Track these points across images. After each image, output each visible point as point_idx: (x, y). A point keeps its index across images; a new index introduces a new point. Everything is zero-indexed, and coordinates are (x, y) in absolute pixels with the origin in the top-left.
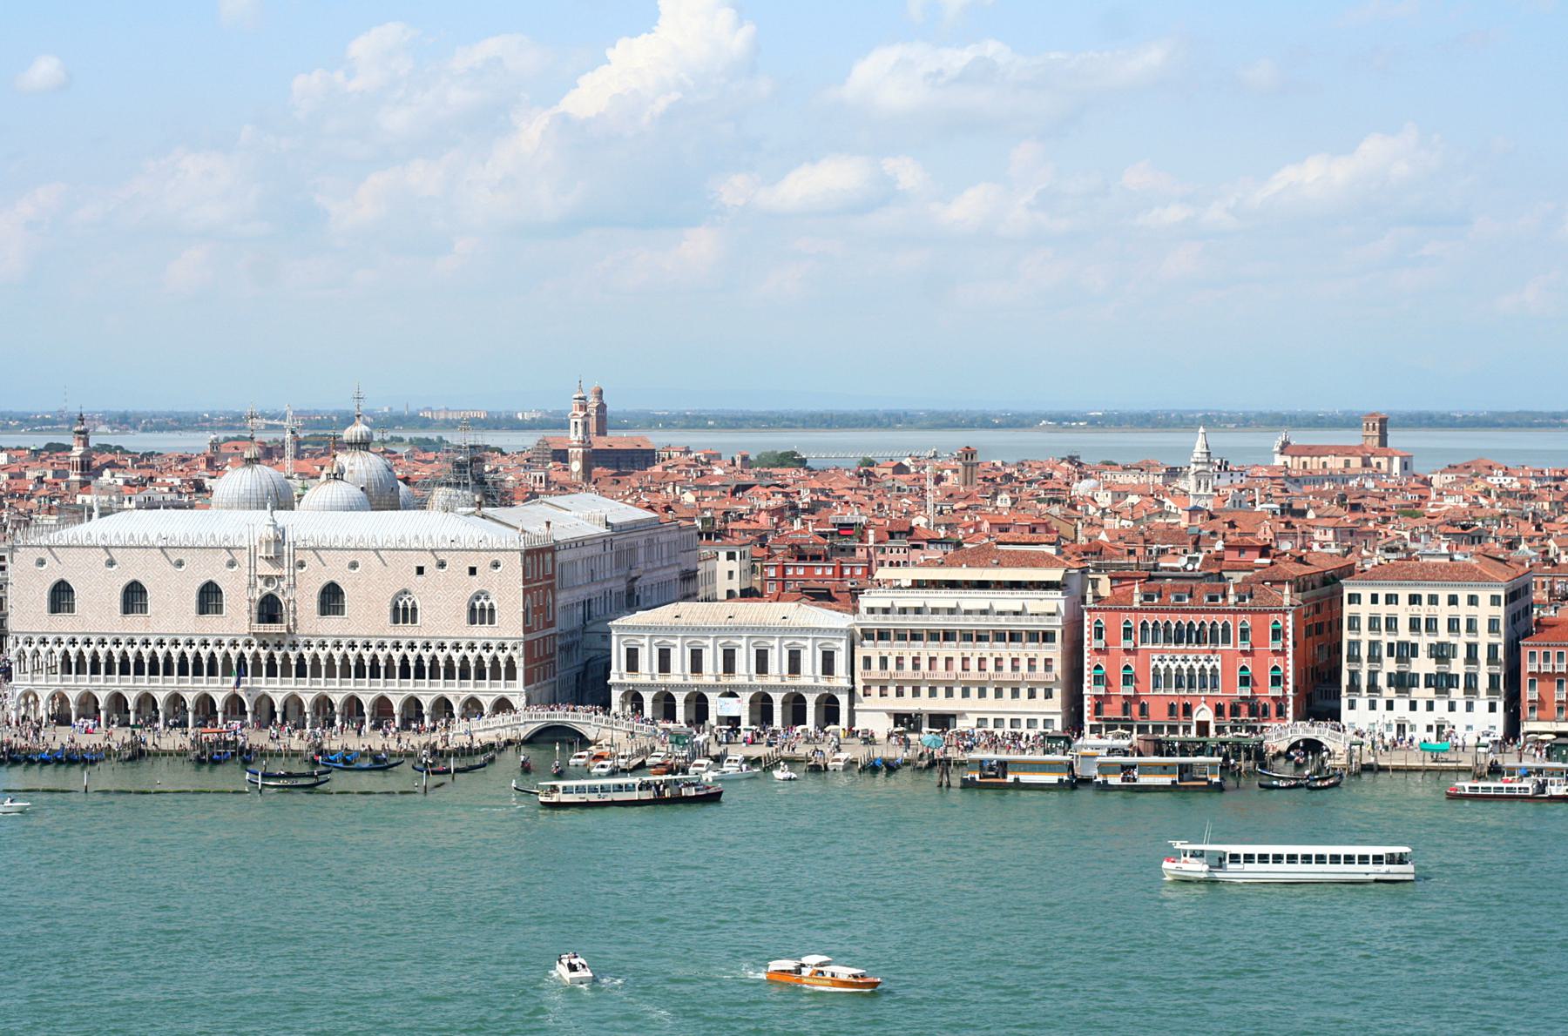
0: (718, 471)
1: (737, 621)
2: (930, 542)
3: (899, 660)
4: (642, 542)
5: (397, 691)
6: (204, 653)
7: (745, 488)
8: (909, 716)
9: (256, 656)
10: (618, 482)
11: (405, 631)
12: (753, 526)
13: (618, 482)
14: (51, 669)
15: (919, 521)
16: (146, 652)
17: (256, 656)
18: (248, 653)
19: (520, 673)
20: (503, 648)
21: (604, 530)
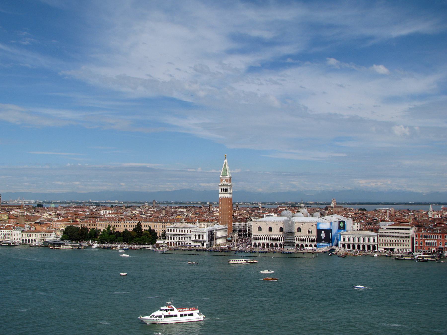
1: (360, 234)
3: (385, 240)
11: (310, 234)
14: (258, 239)
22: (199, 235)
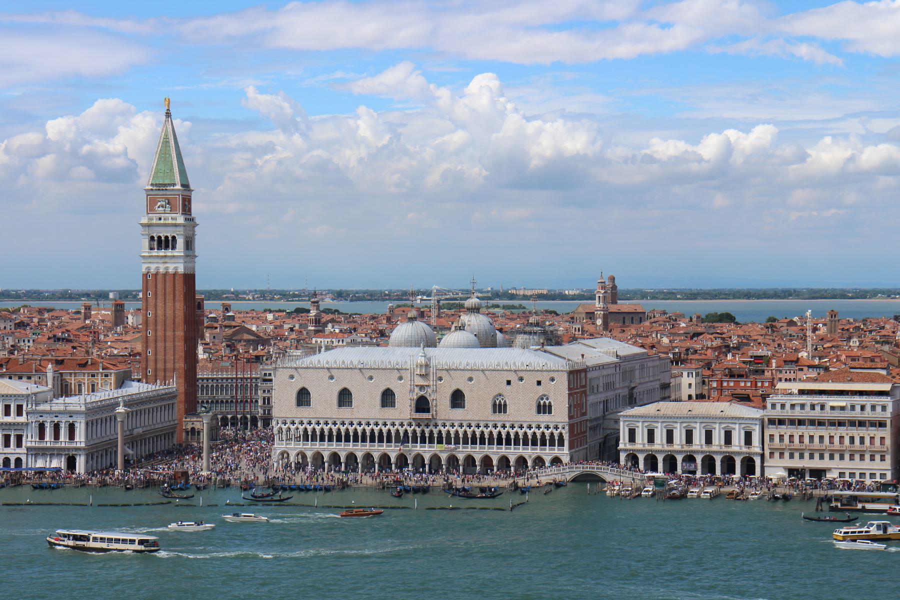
0: (683, 325)
1: (694, 413)
2: (809, 367)
3: (791, 436)
4: (637, 367)
5: (495, 452)
6: (385, 430)
7: (699, 334)
8: (797, 470)
9: (414, 432)
10: (624, 331)
11: (500, 418)
12: (703, 357)
13: (624, 331)
14: (298, 439)
15: (803, 354)
16: (351, 429)
17: (414, 432)
18: (410, 430)
19: (566, 443)
20: (556, 428)
21: (615, 360)
22: (57, 428)
